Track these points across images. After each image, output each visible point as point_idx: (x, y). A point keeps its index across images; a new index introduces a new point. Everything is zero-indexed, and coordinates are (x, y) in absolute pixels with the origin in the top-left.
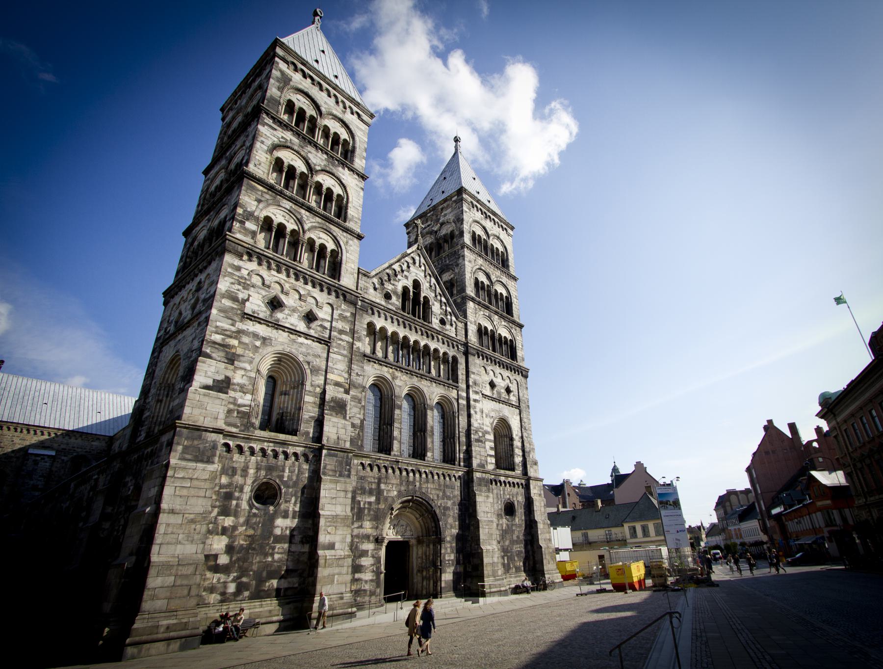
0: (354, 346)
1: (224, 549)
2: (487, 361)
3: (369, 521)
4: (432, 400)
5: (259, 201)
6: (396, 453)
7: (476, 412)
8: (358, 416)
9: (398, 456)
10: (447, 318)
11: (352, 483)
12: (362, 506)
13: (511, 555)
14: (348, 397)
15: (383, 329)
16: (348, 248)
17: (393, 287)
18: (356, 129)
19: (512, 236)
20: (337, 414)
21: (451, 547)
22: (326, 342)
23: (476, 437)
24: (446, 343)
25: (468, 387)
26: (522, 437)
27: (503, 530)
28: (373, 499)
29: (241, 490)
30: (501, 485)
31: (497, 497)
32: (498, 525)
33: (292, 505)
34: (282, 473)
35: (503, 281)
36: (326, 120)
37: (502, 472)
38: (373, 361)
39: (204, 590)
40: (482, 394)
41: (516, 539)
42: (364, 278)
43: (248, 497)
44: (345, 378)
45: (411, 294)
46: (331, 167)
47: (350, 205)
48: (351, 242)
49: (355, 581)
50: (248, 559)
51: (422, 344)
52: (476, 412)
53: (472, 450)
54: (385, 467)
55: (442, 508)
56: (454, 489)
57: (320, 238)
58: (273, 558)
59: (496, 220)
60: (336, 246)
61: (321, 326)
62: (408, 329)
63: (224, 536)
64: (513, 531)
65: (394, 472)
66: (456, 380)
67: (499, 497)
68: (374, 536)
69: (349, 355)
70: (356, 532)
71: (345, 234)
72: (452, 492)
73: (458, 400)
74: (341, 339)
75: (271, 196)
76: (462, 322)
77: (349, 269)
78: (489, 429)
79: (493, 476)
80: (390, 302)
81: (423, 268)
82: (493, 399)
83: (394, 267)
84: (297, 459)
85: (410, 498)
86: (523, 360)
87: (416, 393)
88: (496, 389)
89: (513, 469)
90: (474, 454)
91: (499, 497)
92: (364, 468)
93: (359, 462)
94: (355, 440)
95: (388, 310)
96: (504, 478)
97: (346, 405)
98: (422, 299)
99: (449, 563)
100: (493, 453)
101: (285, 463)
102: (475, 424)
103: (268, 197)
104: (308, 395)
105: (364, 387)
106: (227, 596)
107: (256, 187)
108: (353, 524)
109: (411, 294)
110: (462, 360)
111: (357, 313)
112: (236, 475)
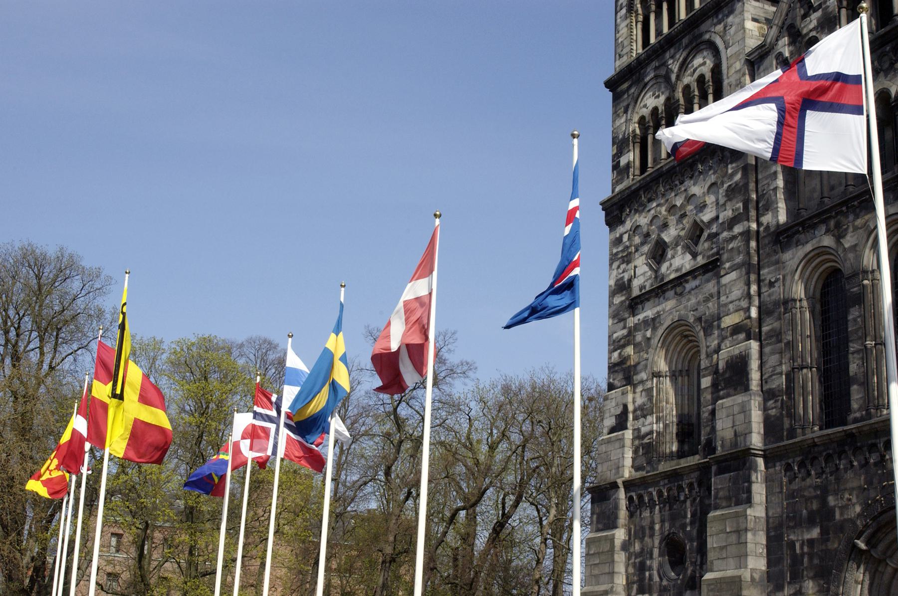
3: (813, 578)
12: (798, 551)
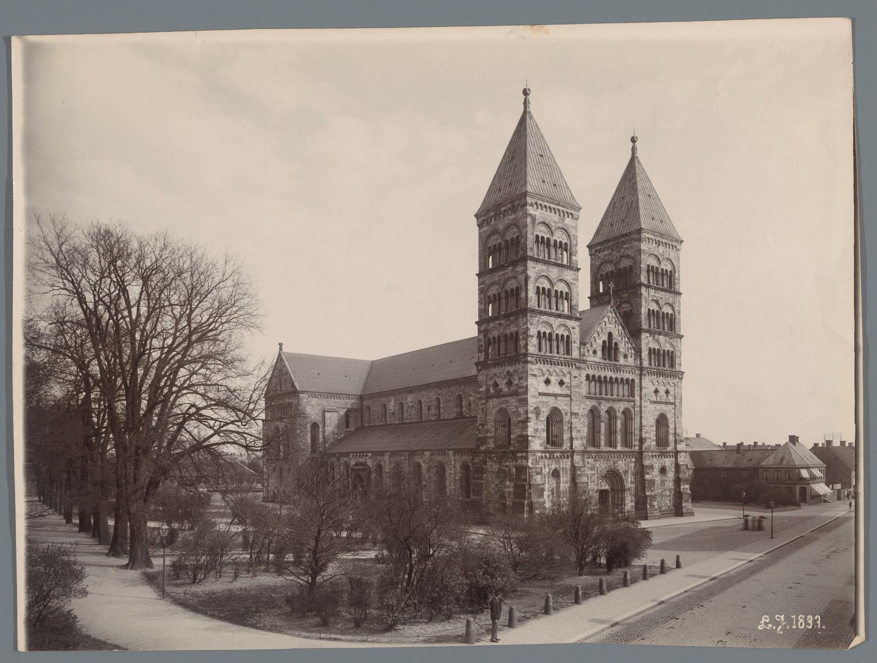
66: (633, 395)
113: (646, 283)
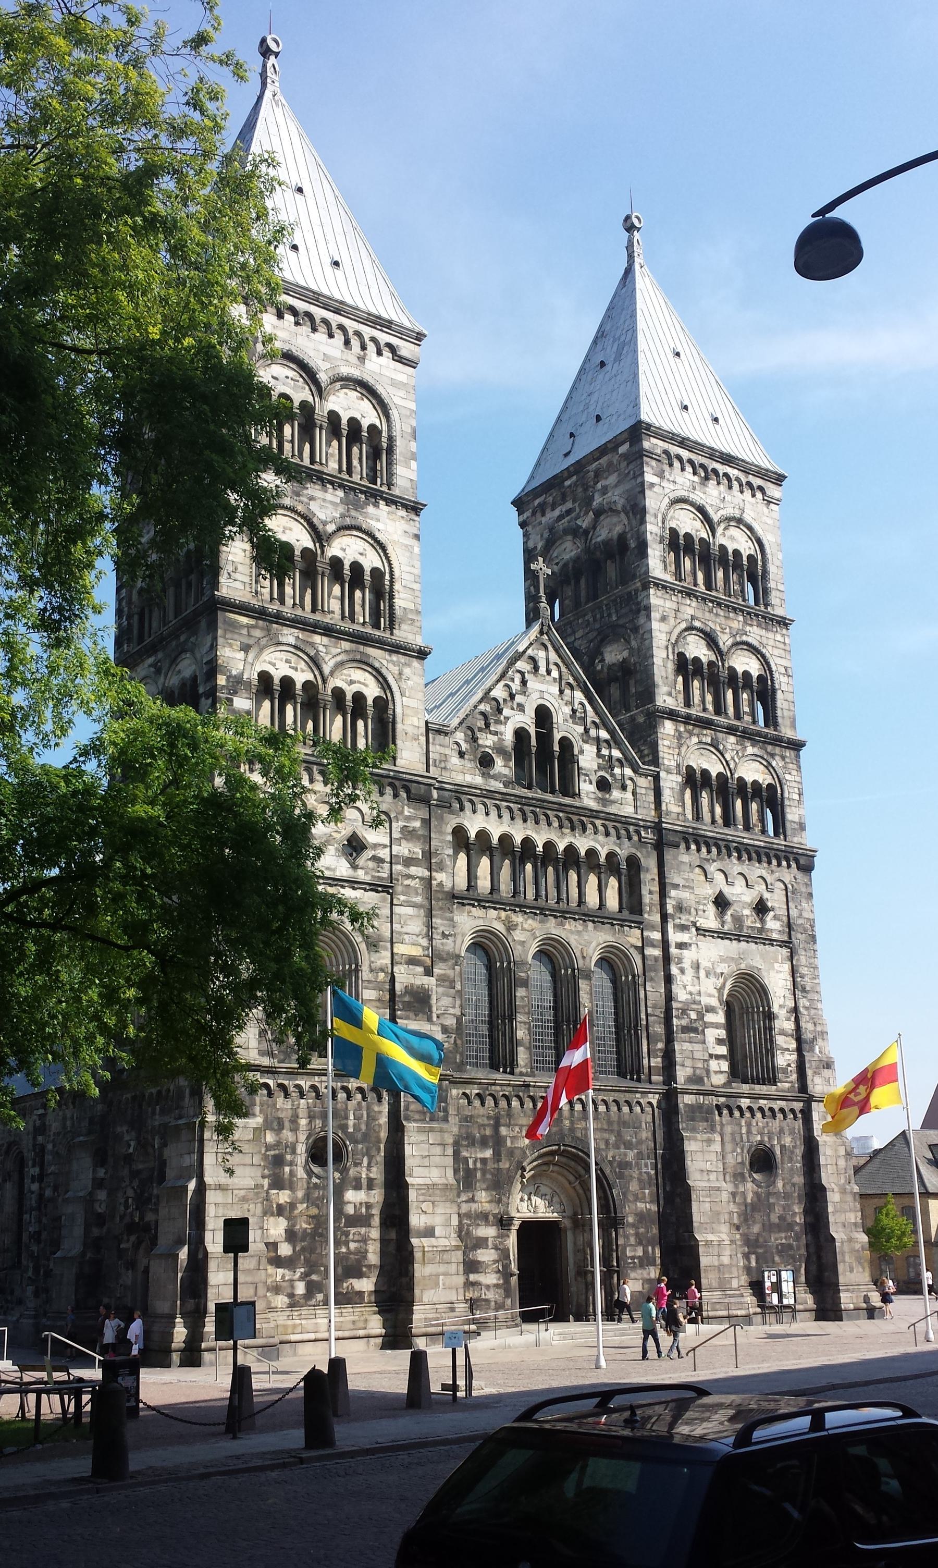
0: (434, 882)
1: (284, 1235)
2: (709, 852)
3: (486, 1190)
4: (587, 960)
5: (246, 648)
6: (524, 1070)
7: (682, 971)
8: (451, 1011)
9: (527, 1075)
10: (613, 775)
11: (453, 1127)
12: (471, 1166)
13: (765, 1252)
14: (432, 980)
15: (483, 835)
16: (403, 686)
17: (495, 738)
18: (391, 389)
19: (777, 502)
20: (416, 1015)
21: (637, 1235)
22: (385, 887)
23: (684, 1022)
24: (612, 831)
25: (664, 917)
26: (795, 1010)
27: (746, 1205)
28: (488, 1153)
29: (294, 1152)
30: (742, 1115)
31: (734, 1139)
32: (734, 1194)
33: (364, 1169)
34: (345, 1121)
35: (750, 640)
36: (332, 398)
37: (745, 1088)
38: (469, 904)
39: (268, 1290)
40: (698, 929)
41: (777, 1221)
42: (440, 738)
43: (303, 1161)
44: (423, 947)
45: (534, 741)
46: (353, 513)
47: (397, 587)
48: (407, 671)
49: (469, 1284)
50: (316, 1249)
51: (561, 847)
52: (682, 971)
53: (674, 1051)
54: (504, 1095)
55: (615, 1165)
56: (640, 1127)
57: (352, 682)
58: (348, 1248)
59: (733, 472)
60: (383, 688)
61: (374, 858)
62: (530, 822)
63: (281, 1218)
64: (771, 1207)
65: (522, 1105)
67: (738, 1139)
68: (495, 1215)
69: (426, 903)
70: (465, 1208)
71: (395, 657)
72: (636, 1133)
73: (641, 950)
74: (409, 876)
75: (262, 629)
76: (646, 776)
77: (410, 730)
78: (714, 1002)
79: (722, 1100)
80: (492, 773)
81: (555, 674)
82: (722, 935)
83: (493, 693)
84: (364, 1098)
85: (554, 1148)
86: (802, 827)
87: (554, 947)
88: (729, 913)
89: (773, 1081)
90: (679, 1058)
91: (738, 1139)
92: (469, 1103)
93: (461, 1092)
94: (451, 1055)
95: (489, 794)
96: (748, 1101)
97: (429, 997)
98: (556, 748)
99: (635, 1263)
100: (723, 1050)
101: (347, 1105)
102: (681, 995)
103: (257, 633)
104: (367, 988)
105: (458, 956)
106: (297, 1298)
107: (236, 621)
108: (459, 1196)
109: (534, 741)
110: (649, 862)
111: (433, 814)
112: (283, 1129)
113: (669, 578)
